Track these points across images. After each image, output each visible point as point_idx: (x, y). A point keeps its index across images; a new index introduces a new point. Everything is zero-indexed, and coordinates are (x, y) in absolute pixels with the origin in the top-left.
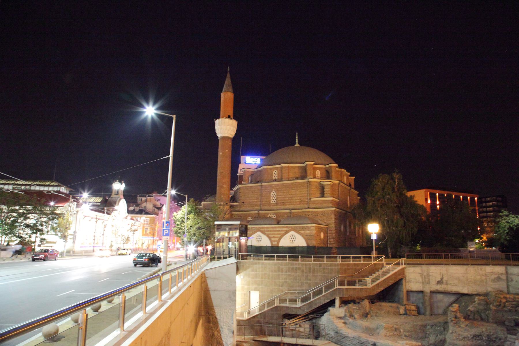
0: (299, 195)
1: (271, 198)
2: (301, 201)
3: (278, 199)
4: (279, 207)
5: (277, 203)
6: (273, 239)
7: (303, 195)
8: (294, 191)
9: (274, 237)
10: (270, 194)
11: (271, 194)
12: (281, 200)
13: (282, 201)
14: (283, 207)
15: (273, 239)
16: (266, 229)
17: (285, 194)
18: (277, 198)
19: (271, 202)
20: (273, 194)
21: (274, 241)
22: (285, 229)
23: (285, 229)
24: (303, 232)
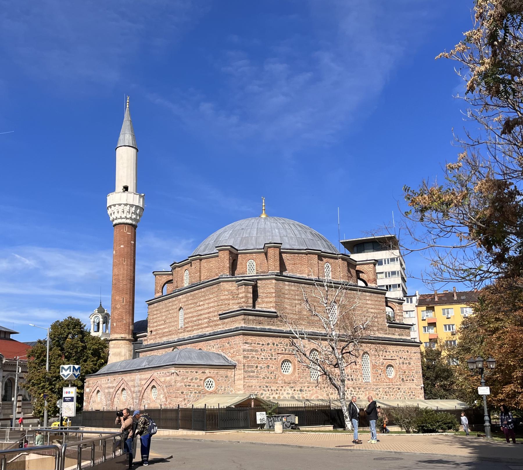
2: (209, 322)
7: (211, 310)
8: (201, 303)
17: (192, 310)
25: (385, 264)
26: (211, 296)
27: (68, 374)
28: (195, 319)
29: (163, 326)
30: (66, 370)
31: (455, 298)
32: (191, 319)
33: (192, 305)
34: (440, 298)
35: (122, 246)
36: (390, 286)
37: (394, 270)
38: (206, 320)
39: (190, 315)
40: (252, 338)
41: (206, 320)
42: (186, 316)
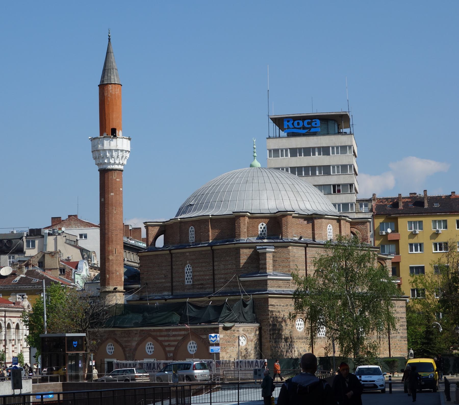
0: (223, 272)
1: (186, 275)
3: (195, 278)
4: (196, 291)
5: (193, 285)
6: (167, 349)
9: (169, 346)
10: (183, 268)
11: (186, 269)
12: (199, 280)
13: (202, 282)
14: (201, 291)
15: (167, 349)
16: (158, 334)
18: (193, 276)
19: (186, 283)
20: (188, 269)
21: (170, 352)
22: (183, 333)
23: (183, 333)
24: (204, 337)
25: (333, 153)
26: (228, 258)
27: (215, 340)
28: (208, 278)
29: (163, 281)
30: (213, 337)
31: (426, 206)
32: (203, 277)
33: (204, 264)
34: (406, 204)
35: (112, 194)
36: (339, 185)
37: (344, 163)
38: (223, 280)
39: (202, 273)
40: (275, 301)
41: (223, 280)
42: (195, 274)
